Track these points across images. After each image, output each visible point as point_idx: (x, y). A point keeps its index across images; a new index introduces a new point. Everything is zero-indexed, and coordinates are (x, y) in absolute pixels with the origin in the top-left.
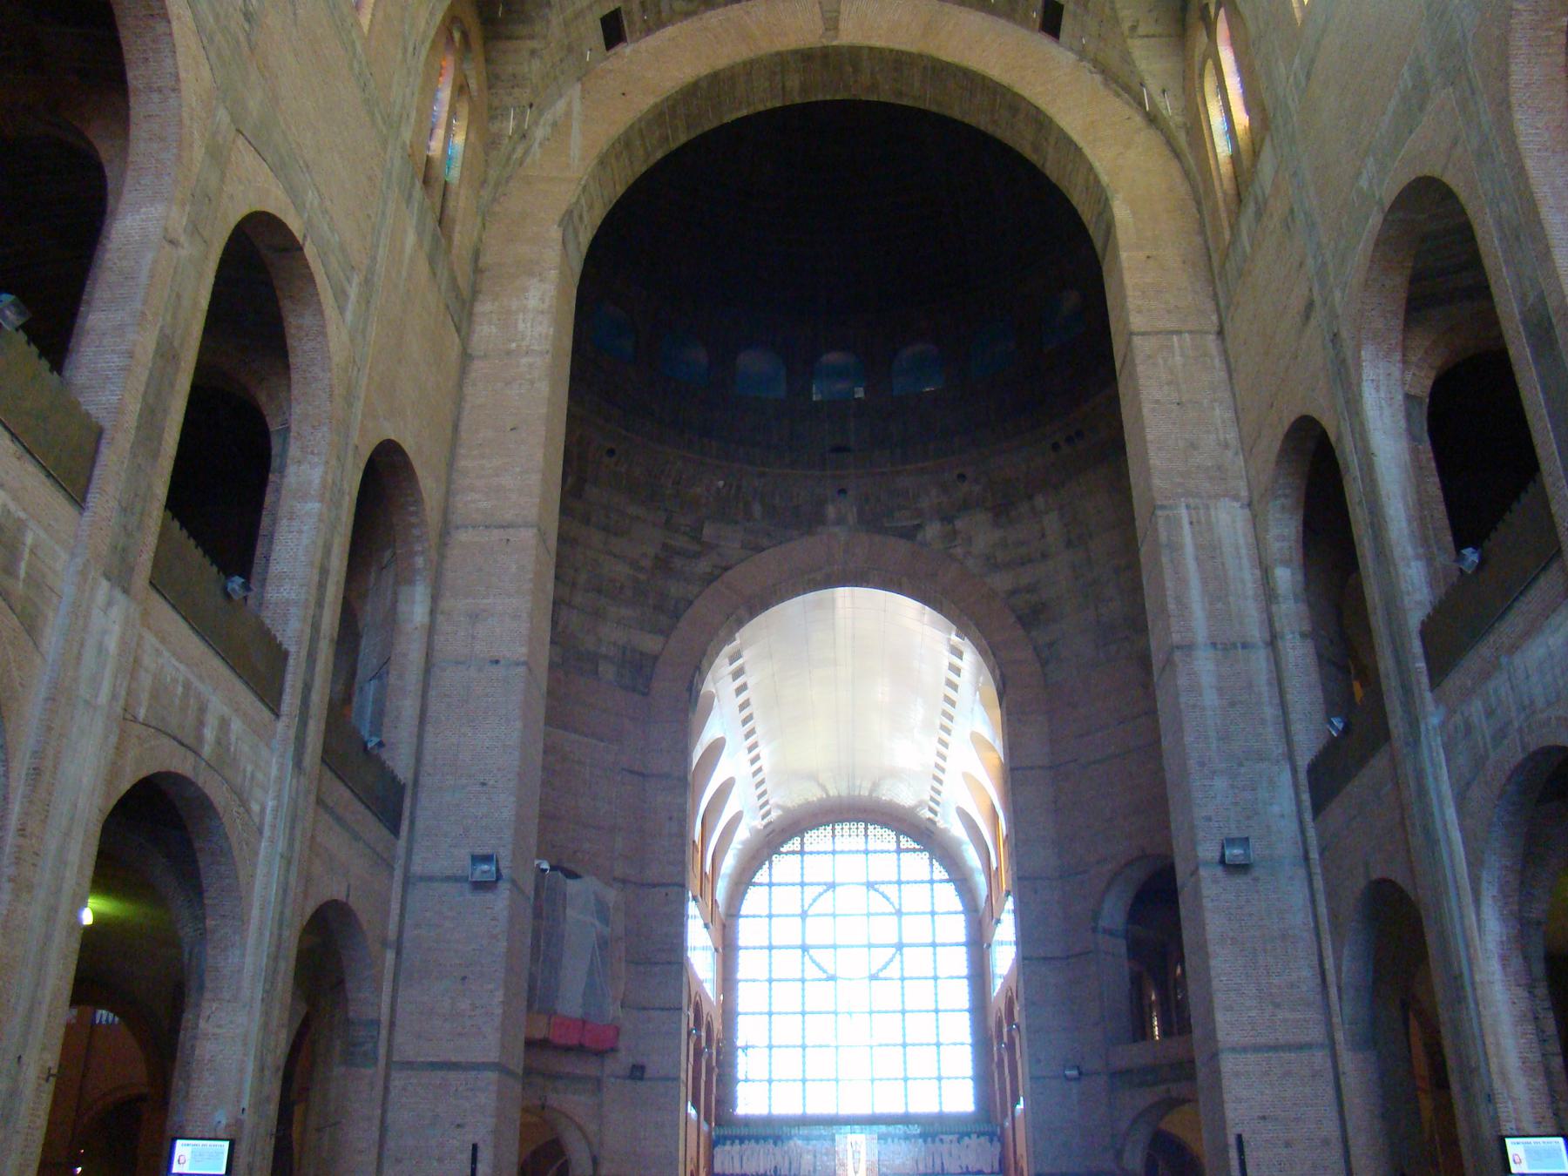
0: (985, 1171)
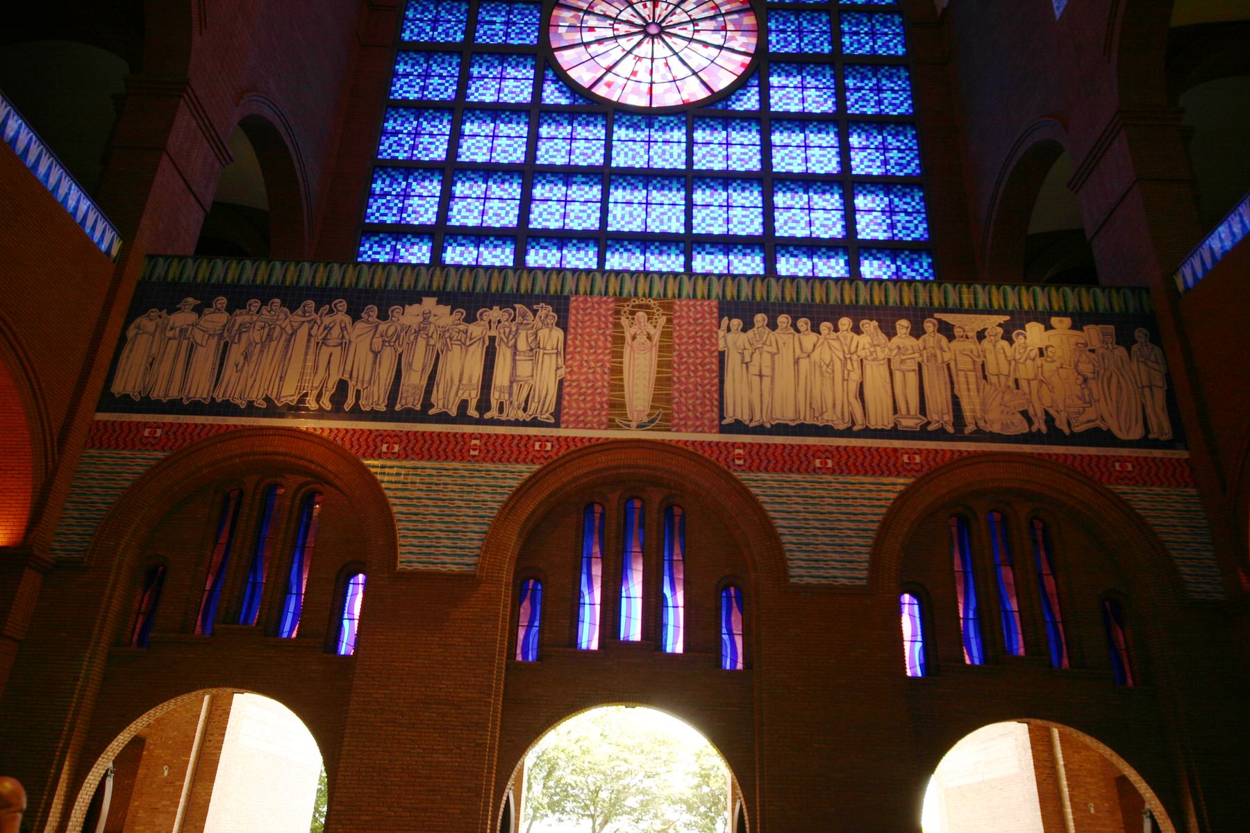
0: (1122, 436)
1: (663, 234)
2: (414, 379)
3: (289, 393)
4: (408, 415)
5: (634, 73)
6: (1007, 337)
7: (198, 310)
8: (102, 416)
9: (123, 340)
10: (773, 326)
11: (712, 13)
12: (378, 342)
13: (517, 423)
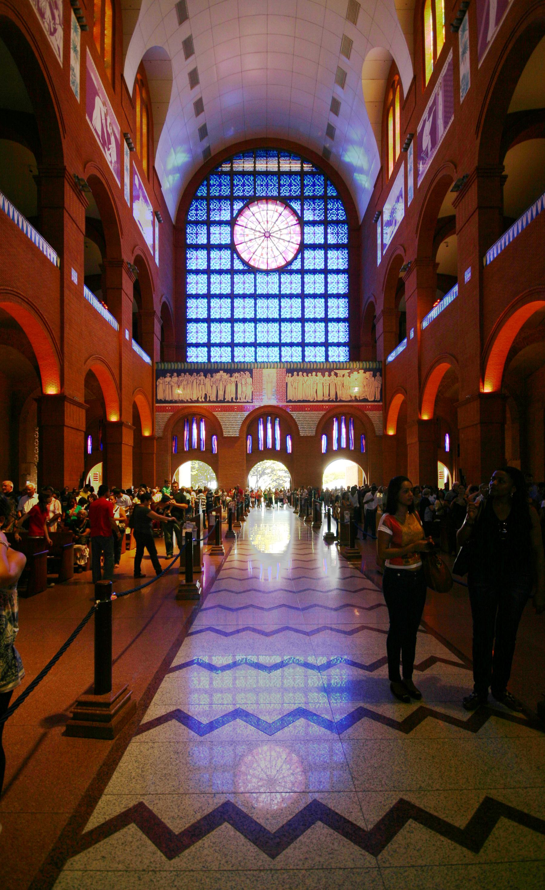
0: (370, 400)
1: (273, 343)
2: (221, 393)
3: (195, 398)
4: (221, 402)
5: (262, 255)
6: (349, 376)
7: (171, 377)
8: (157, 405)
9: (156, 386)
10: (298, 375)
11: (286, 226)
12: (212, 383)
13: (244, 402)
